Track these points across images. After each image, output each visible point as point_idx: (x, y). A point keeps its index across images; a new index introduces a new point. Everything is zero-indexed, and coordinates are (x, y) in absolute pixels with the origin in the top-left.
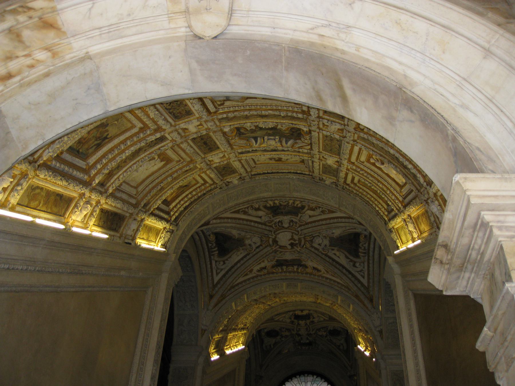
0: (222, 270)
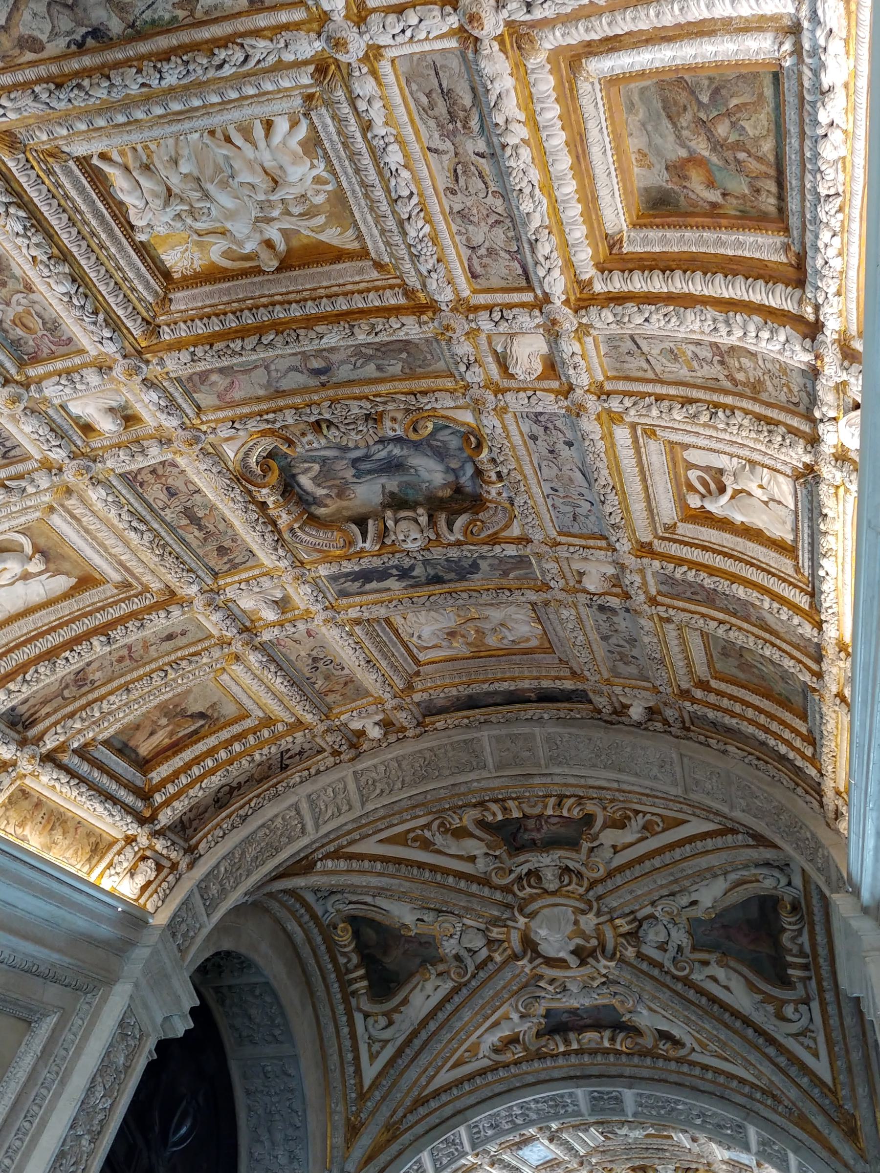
0: (387, 1042)
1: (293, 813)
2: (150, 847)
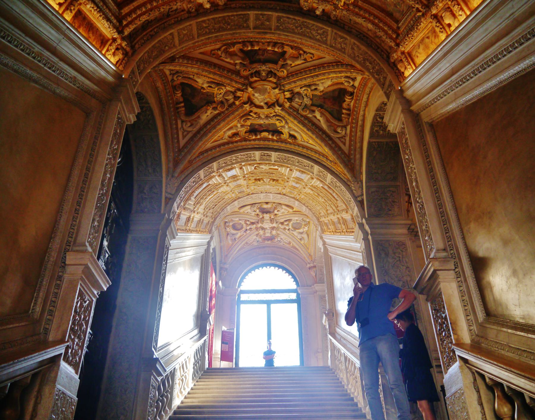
1: (171, 37)
2: (120, 45)
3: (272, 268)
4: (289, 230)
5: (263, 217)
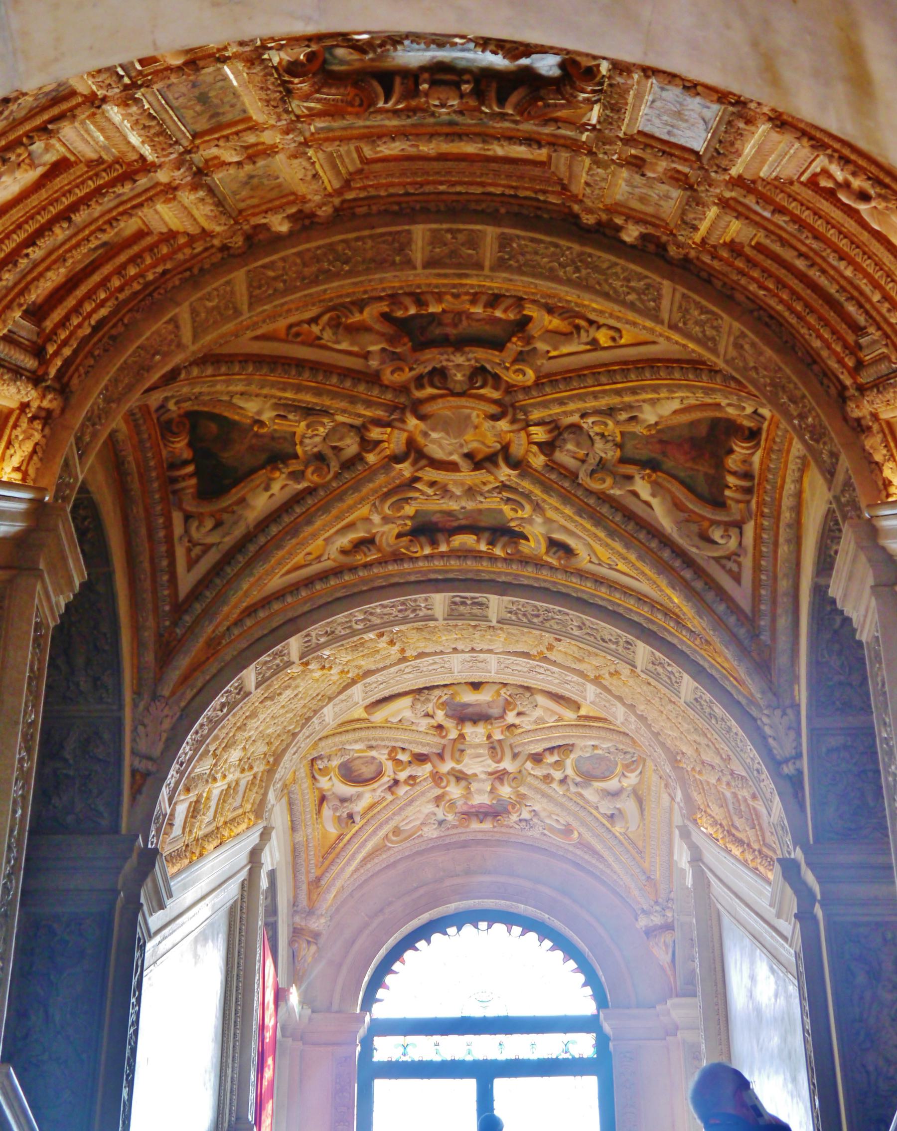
3: (499, 928)
4: (563, 781)
5: (462, 736)
